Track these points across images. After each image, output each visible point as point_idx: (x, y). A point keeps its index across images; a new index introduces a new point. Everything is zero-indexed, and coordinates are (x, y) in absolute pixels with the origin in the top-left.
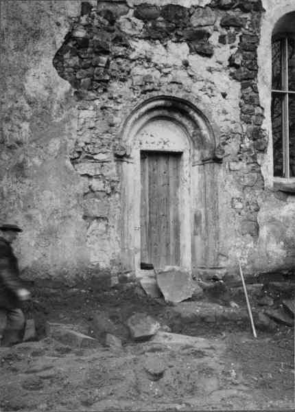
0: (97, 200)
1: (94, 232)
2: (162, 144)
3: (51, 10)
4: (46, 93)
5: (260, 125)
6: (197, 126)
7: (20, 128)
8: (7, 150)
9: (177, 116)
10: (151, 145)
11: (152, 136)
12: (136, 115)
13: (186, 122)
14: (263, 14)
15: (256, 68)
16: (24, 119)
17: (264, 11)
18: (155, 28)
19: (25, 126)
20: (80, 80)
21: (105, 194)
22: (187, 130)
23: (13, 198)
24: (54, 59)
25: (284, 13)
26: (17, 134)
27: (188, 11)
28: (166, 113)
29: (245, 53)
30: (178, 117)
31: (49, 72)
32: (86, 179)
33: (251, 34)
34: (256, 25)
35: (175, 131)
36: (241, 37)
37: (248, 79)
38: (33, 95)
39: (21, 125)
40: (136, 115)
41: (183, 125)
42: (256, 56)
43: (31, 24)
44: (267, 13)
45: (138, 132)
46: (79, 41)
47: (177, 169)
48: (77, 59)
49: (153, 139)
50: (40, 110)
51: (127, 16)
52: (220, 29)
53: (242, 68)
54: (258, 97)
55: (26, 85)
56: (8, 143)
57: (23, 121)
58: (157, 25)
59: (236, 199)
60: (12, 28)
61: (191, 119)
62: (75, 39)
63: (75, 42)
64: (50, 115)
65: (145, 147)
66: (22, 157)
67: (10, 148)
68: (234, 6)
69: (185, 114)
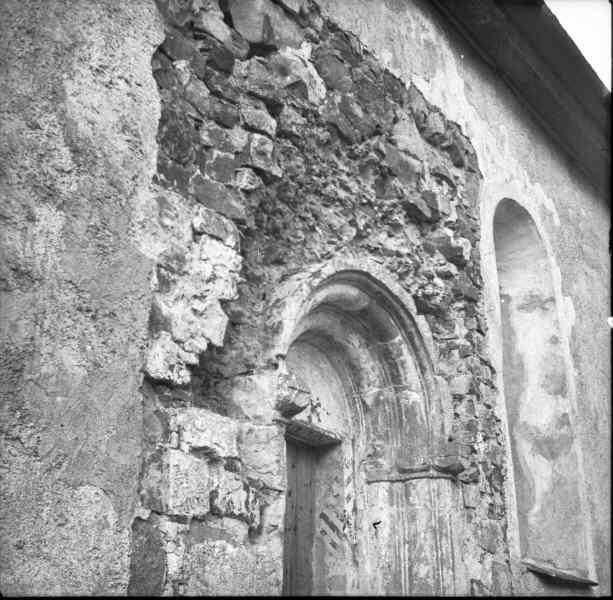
0: (230, 549)
7: (31, 219)
9: (356, 346)
16: (50, 194)
19: (50, 218)
20: (207, 148)
22: (359, 385)
26: (18, 236)
30: (356, 343)
39: (37, 211)
41: (354, 369)
50: (101, 186)
57: (44, 200)
61: (387, 358)
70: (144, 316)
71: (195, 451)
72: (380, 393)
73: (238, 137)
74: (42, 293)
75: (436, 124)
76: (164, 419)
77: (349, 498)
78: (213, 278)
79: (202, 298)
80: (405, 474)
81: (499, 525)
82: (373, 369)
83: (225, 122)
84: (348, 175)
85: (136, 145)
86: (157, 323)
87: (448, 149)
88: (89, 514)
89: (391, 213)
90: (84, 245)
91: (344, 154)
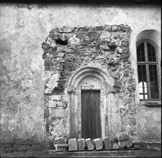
0: (59, 110)
1: (58, 124)
2: (91, 87)
3: (42, 38)
4: (39, 69)
5: (132, 77)
6: (104, 79)
7: (28, 82)
8: (23, 91)
9: (96, 75)
10: (86, 87)
11: (86, 84)
12: (77, 75)
13: (99, 77)
14: (131, 32)
15: (129, 54)
16: (30, 79)
17: (132, 31)
18: (84, 41)
19: (30, 81)
20: (53, 63)
21: (62, 108)
23: (24, 110)
24: (43, 56)
25: (141, 31)
26: (27, 84)
27: (99, 34)
28: (91, 74)
29: (124, 48)
30: (96, 75)
31: (41, 61)
32: (55, 102)
33: (127, 40)
34: (129, 37)
35: (97, 81)
36: (122, 42)
37: (126, 58)
38: (34, 70)
40: (77, 75)
41: (99, 79)
42: (129, 49)
43: (34, 44)
44: (133, 32)
45: (80, 82)
46: (53, 48)
47: (99, 97)
48: (52, 55)
49: (86, 85)
51: (73, 37)
52: (113, 39)
53: (123, 54)
54: (131, 66)
55: (31, 66)
56: (23, 88)
57: (30, 80)
58: (85, 40)
59: (123, 109)
60: (27, 45)
61: (102, 76)
62: (51, 47)
63: (51, 49)
64: (41, 77)
65: (83, 88)
66: (28, 94)
67: (24, 90)
68: (118, 30)
69: (99, 74)
70: (44, 87)
71: (53, 100)
72: (104, 81)
73: (58, 59)
74: (30, 89)
75: (116, 28)
76: (48, 98)
77: (102, 98)
78: (55, 79)
79: (53, 82)
81: (133, 98)
82: (102, 78)
83: (56, 58)
84: (89, 50)
85: (41, 68)
86: (46, 87)
87: (120, 30)
88: (38, 110)
89: (101, 51)
90: (35, 82)
91: (87, 47)
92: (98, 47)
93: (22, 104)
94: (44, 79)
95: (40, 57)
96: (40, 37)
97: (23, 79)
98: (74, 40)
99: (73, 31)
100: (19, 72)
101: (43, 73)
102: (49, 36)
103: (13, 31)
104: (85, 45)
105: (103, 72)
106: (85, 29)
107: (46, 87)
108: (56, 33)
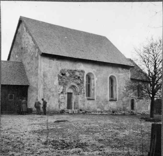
16: (54, 88)
18: (71, 75)
19: (54, 89)
34: (84, 74)
80: (76, 94)
86: (59, 91)
92: (74, 78)
93: (51, 97)
94: (58, 88)
95: (57, 80)
96: (57, 72)
97: (52, 88)
98: (68, 74)
99: (67, 71)
100: (50, 85)
101: (58, 86)
102: (60, 72)
103: (48, 69)
104: (71, 76)
105: (76, 87)
106: (71, 70)
107: (59, 91)
108: (62, 71)
